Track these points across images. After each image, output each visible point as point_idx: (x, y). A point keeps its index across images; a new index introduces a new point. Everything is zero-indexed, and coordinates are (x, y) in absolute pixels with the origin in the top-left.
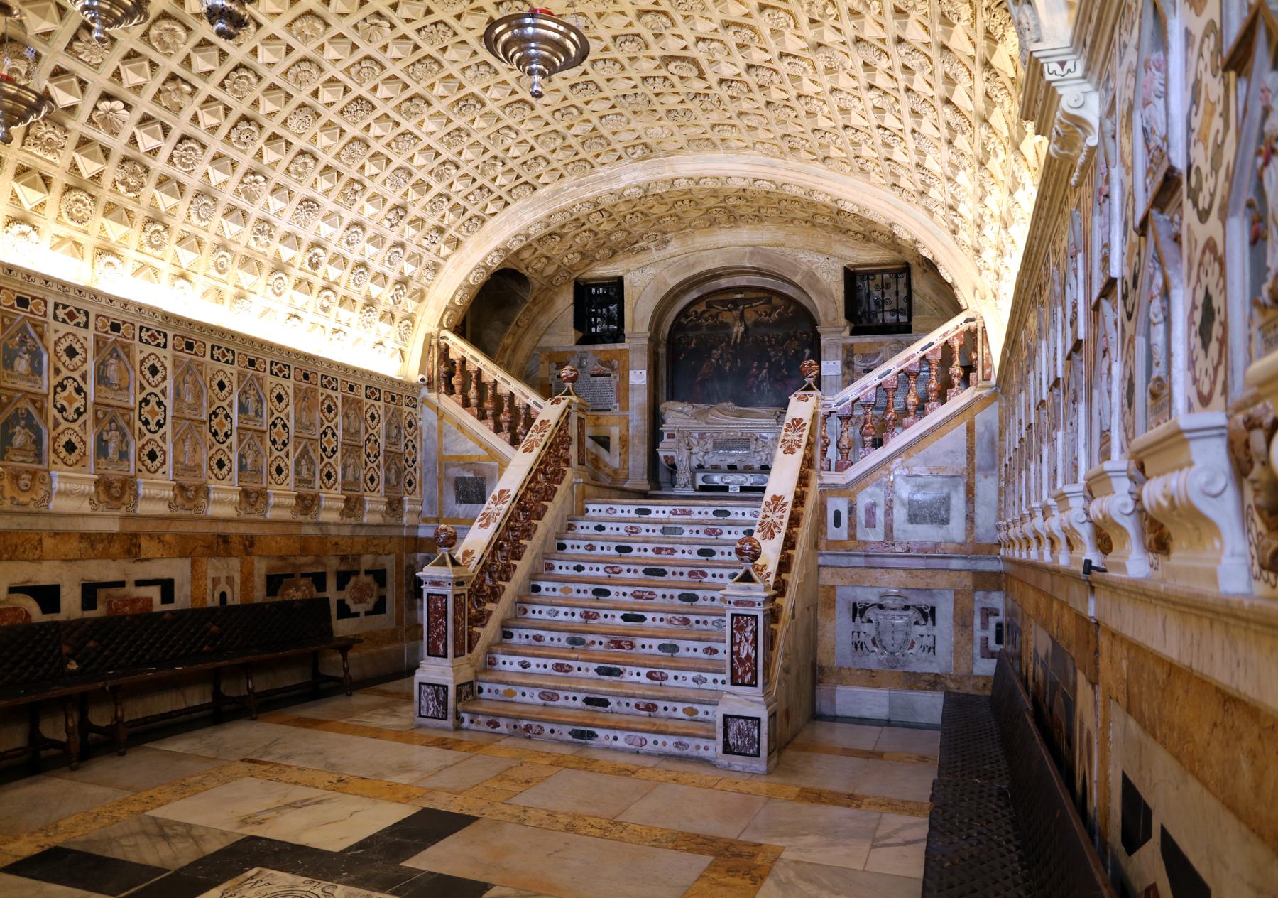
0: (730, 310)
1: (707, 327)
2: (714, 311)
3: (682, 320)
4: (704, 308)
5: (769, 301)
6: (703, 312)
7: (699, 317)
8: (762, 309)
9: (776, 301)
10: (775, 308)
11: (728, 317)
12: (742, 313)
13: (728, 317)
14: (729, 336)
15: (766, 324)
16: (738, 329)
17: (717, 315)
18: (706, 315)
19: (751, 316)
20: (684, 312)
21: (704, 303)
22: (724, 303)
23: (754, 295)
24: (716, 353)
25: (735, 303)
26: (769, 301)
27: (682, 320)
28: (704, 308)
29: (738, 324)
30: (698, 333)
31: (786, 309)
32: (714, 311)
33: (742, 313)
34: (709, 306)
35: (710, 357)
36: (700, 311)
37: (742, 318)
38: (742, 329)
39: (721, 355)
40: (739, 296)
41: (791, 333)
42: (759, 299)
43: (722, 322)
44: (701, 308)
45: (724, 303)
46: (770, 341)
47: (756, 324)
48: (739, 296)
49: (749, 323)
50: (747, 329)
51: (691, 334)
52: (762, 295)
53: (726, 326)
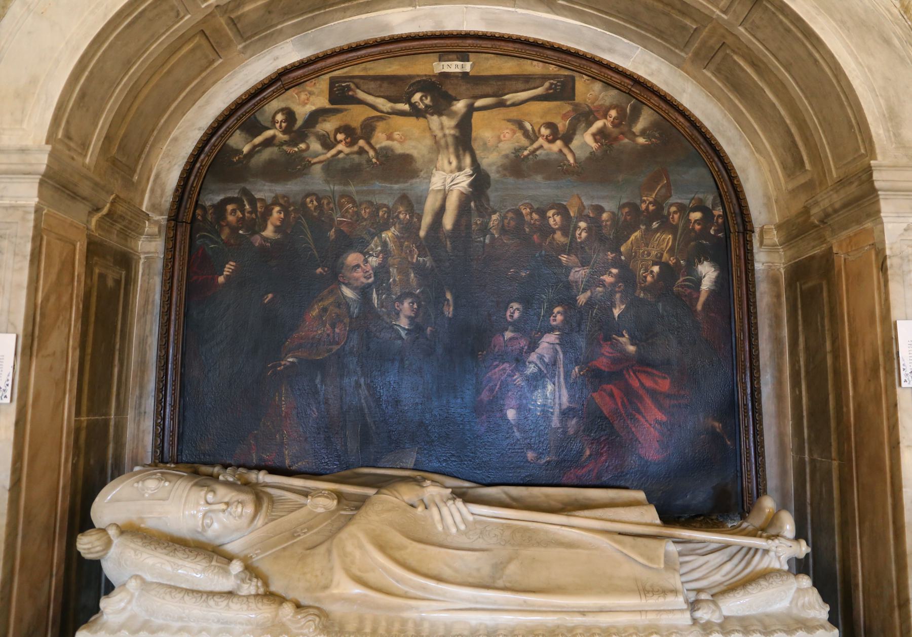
0: (416, 112)
1: (328, 166)
2: (356, 115)
3: (240, 142)
4: (322, 101)
5: (562, 91)
6: (316, 116)
7: (298, 131)
8: (537, 114)
9: (588, 91)
10: (585, 116)
11: (408, 136)
12: (465, 125)
13: (408, 136)
14: (412, 204)
15: (555, 169)
16: (447, 181)
17: (368, 129)
18: (328, 126)
19: (496, 137)
20: (244, 113)
21: (323, 84)
22: (398, 88)
23: (508, 67)
24: (360, 265)
25: (440, 92)
26: (562, 91)
27: (240, 142)
28: (322, 101)
29: (447, 160)
30: (293, 187)
31: (626, 120)
32: (356, 115)
33: (465, 125)
34: (341, 95)
35: (335, 276)
36: (302, 111)
37: (464, 141)
38: (463, 181)
39: (381, 272)
40: (453, 67)
41: (647, 203)
42: (527, 81)
43: (386, 155)
44: (310, 99)
45: (398, 88)
46: (568, 227)
47: (517, 166)
48: (453, 67)
49: (490, 160)
50: (480, 181)
51: (264, 191)
52: (535, 68)
53: (399, 166)
